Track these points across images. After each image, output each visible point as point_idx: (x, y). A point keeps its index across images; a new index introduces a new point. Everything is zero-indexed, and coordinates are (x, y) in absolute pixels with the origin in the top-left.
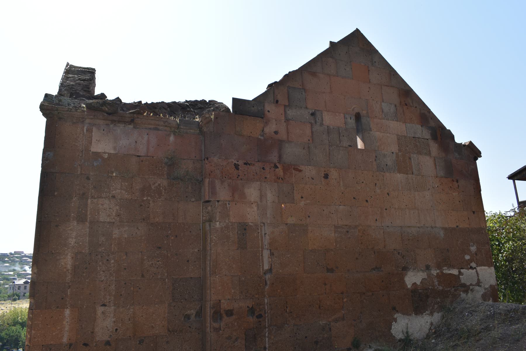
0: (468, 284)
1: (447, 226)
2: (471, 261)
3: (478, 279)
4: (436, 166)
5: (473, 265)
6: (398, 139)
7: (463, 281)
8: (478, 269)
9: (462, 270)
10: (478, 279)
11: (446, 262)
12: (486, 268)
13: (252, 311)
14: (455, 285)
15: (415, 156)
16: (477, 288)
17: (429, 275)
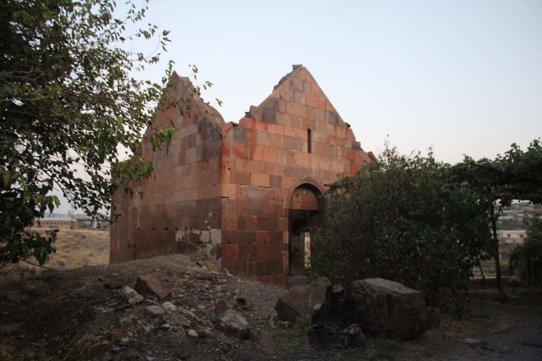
0: (204, 242)
1: (197, 199)
2: (208, 224)
3: (210, 239)
4: (197, 152)
5: (209, 227)
6: (182, 142)
7: (201, 240)
8: (211, 230)
9: (202, 232)
10: (210, 239)
11: (194, 225)
12: (216, 230)
13: (135, 246)
14: (198, 242)
15: (188, 150)
16: (209, 245)
17: (186, 234)
